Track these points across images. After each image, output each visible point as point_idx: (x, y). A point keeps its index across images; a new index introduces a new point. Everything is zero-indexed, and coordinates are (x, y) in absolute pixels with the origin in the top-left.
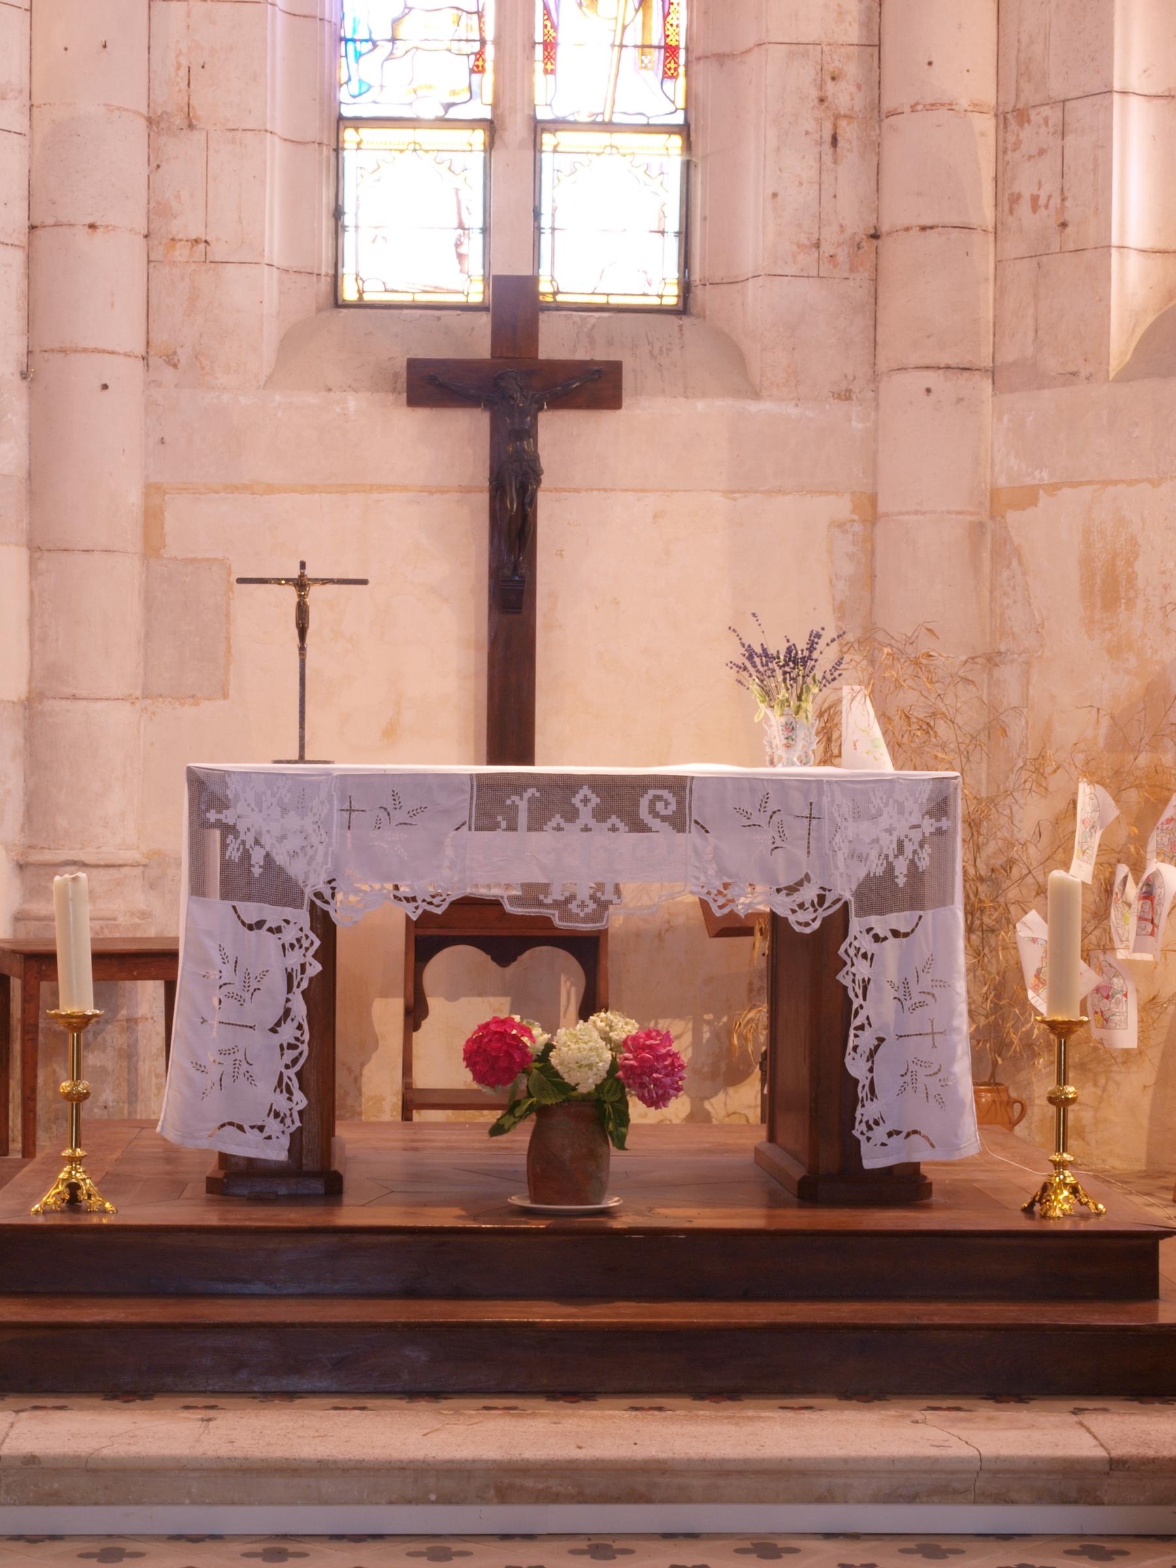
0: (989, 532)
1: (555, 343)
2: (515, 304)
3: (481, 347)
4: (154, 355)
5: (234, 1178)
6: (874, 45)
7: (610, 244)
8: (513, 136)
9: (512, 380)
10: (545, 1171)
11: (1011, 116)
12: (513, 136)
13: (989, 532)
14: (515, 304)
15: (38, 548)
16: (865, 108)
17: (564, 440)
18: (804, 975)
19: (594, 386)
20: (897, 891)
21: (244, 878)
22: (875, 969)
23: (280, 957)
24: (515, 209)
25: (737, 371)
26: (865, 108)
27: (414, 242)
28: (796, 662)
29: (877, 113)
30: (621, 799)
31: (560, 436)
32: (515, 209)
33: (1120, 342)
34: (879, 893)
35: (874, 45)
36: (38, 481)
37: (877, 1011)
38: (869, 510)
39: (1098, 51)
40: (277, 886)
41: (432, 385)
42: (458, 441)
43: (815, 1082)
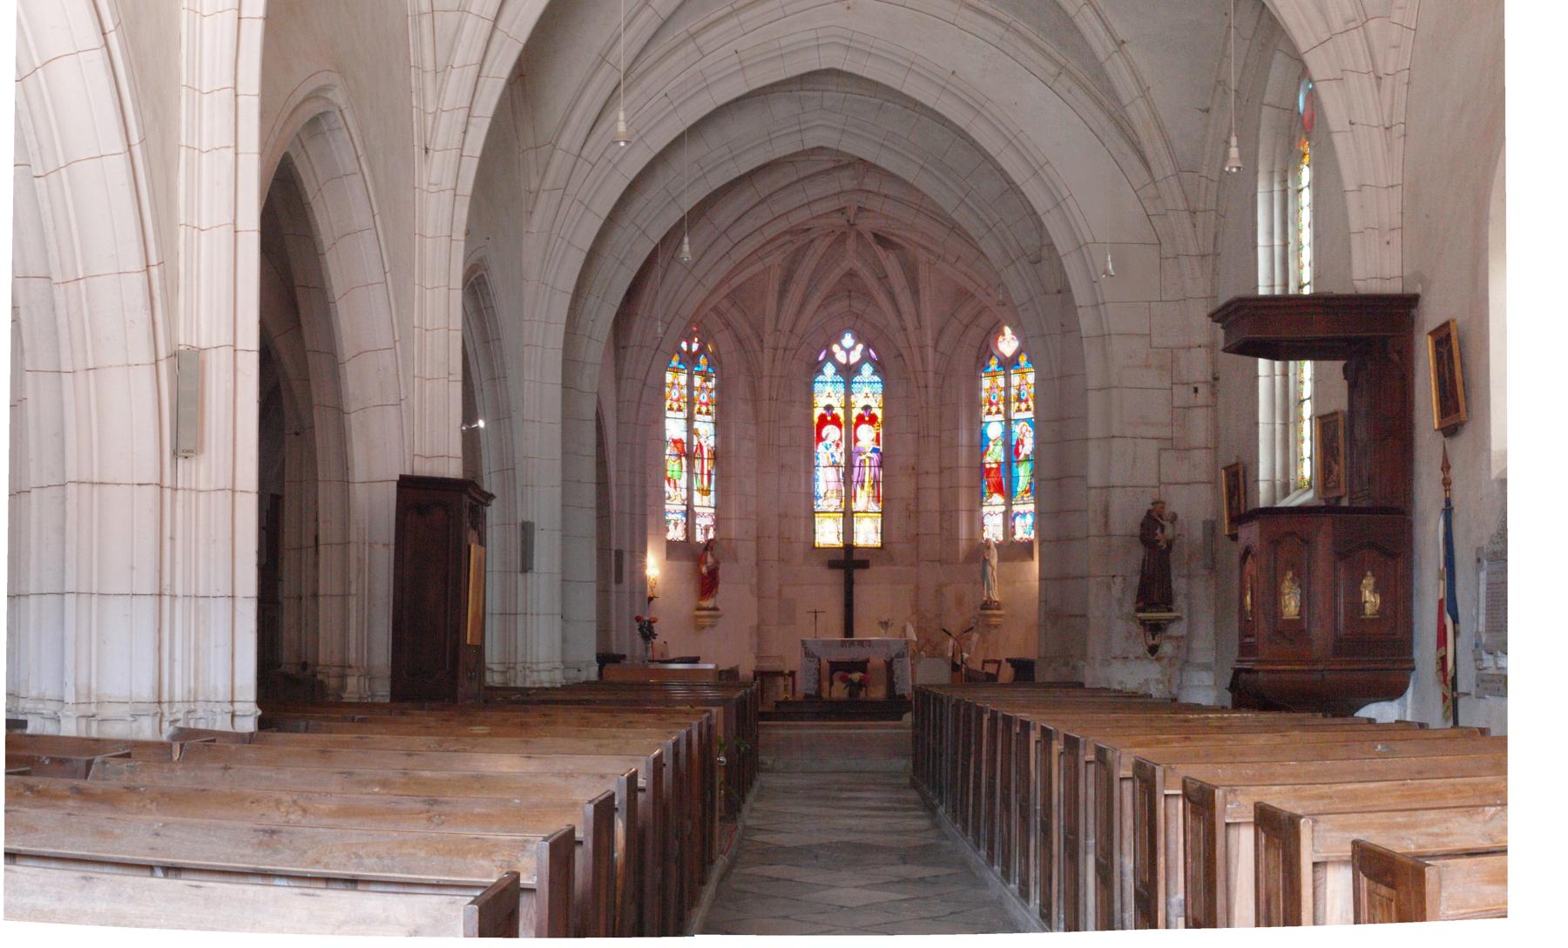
0: (939, 591)
1: (856, 556)
2: (849, 548)
3: (842, 557)
4: (781, 560)
5: (807, 696)
6: (917, 498)
7: (868, 533)
8: (848, 516)
9: (848, 560)
10: (850, 694)
11: (942, 513)
12: (848, 516)
13: (939, 591)
14: (849, 548)
15: (760, 597)
16: (914, 511)
17: (858, 574)
18: (889, 665)
19: (864, 564)
20: (900, 655)
21: (808, 654)
22: (897, 666)
23: (813, 665)
24: (848, 530)
25: (891, 560)
26: (914, 511)
27: (828, 534)
28: (886, 623)
29: (918, 512)
30: (861, 643)
31: (858, 574)
32: (848, 530)
33: (961, 556)
34: (898, 656)
35: (917, 498)
36: (759, 585)
37: (898, 672)
38: (917, 588)
39: (957, 503)
40: (813, 656)
41: (833, 565)
42: (837, 576)
43: (891, 685)
